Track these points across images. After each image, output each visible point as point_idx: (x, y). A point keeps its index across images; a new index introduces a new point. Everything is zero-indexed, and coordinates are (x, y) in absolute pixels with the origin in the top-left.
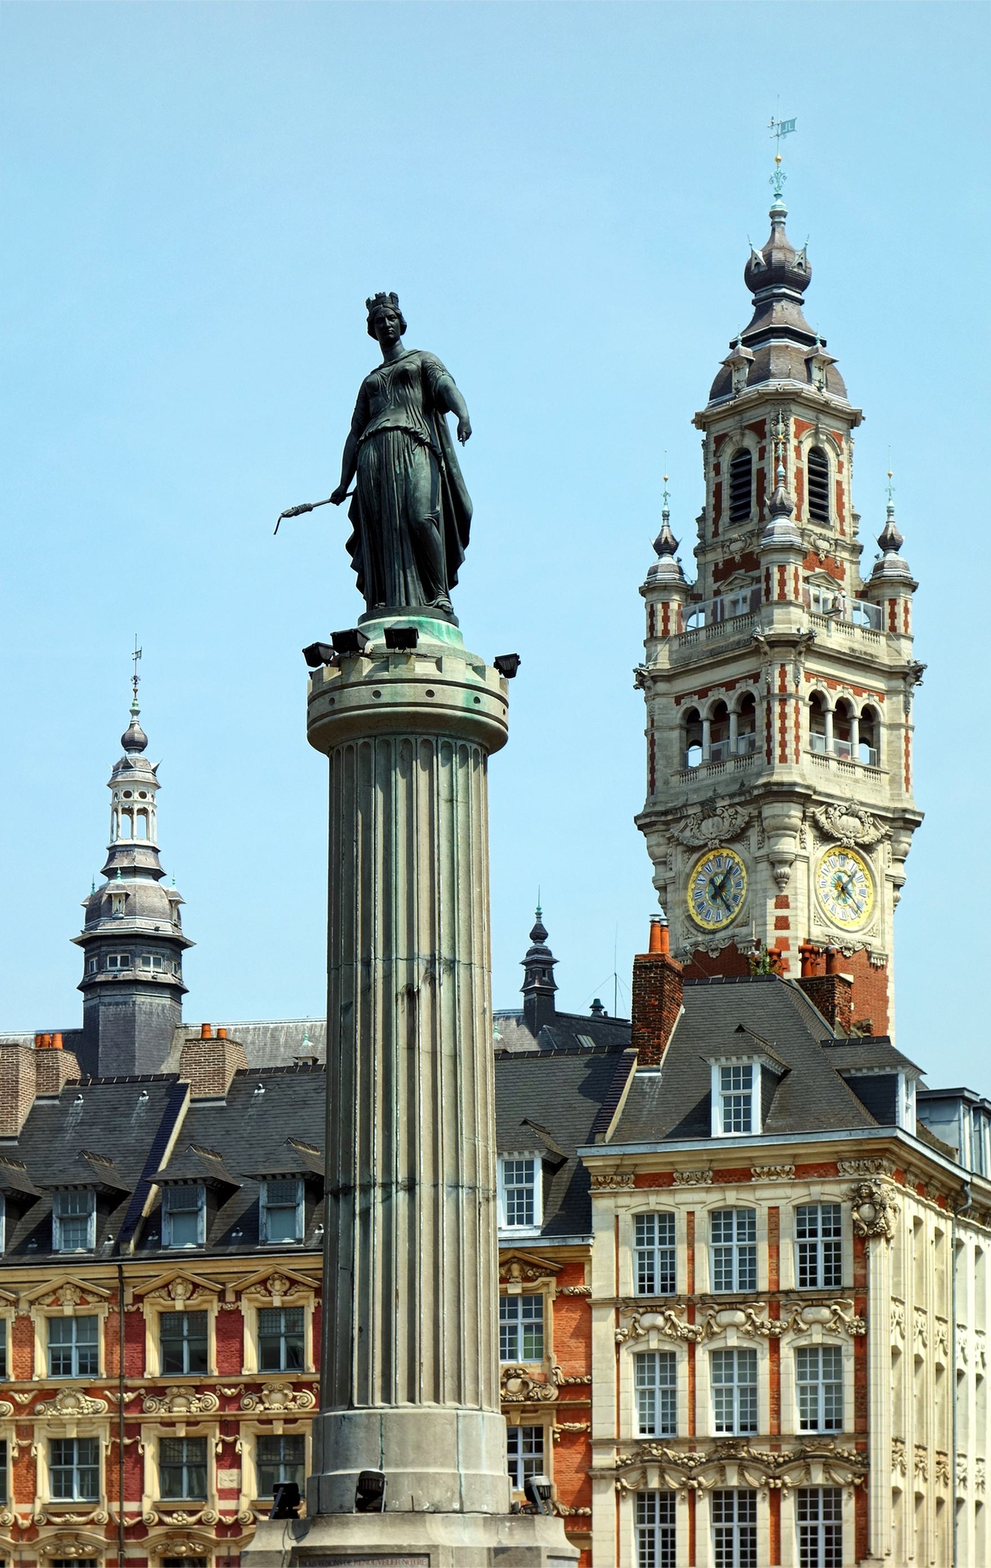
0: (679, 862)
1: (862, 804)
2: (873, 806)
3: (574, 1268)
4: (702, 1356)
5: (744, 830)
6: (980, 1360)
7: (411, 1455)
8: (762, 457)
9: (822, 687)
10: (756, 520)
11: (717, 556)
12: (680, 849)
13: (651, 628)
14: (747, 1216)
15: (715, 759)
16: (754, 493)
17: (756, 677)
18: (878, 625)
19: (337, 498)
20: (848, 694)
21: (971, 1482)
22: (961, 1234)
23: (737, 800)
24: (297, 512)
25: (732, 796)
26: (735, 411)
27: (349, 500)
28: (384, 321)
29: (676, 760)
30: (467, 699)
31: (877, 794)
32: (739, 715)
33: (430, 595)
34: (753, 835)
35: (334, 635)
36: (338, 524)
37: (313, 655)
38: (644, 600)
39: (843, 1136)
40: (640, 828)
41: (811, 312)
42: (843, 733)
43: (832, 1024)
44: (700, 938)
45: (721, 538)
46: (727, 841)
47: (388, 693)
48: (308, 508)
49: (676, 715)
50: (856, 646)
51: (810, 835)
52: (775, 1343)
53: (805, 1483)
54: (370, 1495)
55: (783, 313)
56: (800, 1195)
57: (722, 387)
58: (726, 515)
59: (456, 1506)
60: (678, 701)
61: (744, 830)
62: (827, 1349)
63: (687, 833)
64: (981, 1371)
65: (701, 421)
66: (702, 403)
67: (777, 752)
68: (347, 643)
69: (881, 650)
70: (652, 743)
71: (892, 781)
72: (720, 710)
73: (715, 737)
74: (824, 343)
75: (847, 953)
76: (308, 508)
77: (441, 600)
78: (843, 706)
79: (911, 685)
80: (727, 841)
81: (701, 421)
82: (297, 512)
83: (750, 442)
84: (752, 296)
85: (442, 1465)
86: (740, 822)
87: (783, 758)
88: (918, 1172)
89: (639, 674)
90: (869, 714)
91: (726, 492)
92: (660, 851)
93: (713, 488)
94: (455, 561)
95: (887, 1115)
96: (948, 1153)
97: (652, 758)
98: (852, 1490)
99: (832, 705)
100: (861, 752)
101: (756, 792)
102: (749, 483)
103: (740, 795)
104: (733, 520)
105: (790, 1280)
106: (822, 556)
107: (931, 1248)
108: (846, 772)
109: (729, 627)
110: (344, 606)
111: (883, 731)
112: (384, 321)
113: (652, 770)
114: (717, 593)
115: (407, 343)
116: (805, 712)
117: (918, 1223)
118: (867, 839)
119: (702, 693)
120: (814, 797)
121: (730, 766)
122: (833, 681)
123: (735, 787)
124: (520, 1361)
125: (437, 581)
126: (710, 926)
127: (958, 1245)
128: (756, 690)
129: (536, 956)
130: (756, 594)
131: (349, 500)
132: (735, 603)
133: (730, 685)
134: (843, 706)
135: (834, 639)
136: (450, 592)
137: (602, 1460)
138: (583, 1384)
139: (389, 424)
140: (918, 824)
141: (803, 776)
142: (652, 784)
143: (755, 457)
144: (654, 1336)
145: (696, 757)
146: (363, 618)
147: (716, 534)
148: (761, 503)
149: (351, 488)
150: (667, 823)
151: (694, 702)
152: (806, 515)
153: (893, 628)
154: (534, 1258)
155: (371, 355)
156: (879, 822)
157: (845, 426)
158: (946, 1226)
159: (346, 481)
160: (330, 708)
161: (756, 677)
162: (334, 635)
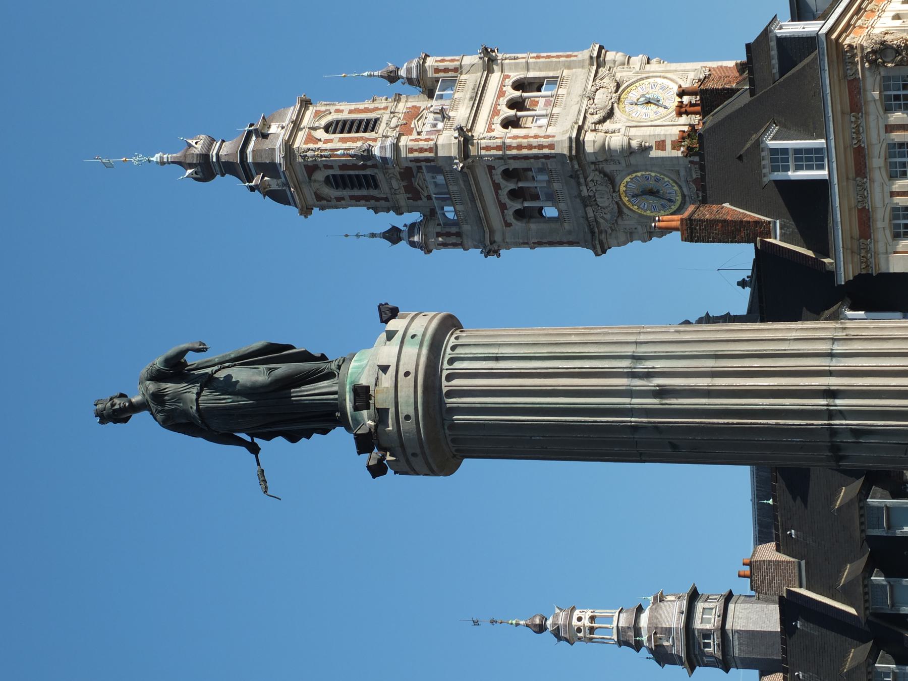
11: (402, 198)
20: (503, 101)
51: (608, 125)
72: (515, 194)
73: (536, 197)
91: (357, 192)
101: (576, 166)
104: (376, 186)
118: (612, 87)
119: (503, 207)
122: (495, 112)
133: (497, 187)
143: (331, 172)
147: (386, 199)
148: (364, 167)
152: (373, 135)
153: (456, 70)
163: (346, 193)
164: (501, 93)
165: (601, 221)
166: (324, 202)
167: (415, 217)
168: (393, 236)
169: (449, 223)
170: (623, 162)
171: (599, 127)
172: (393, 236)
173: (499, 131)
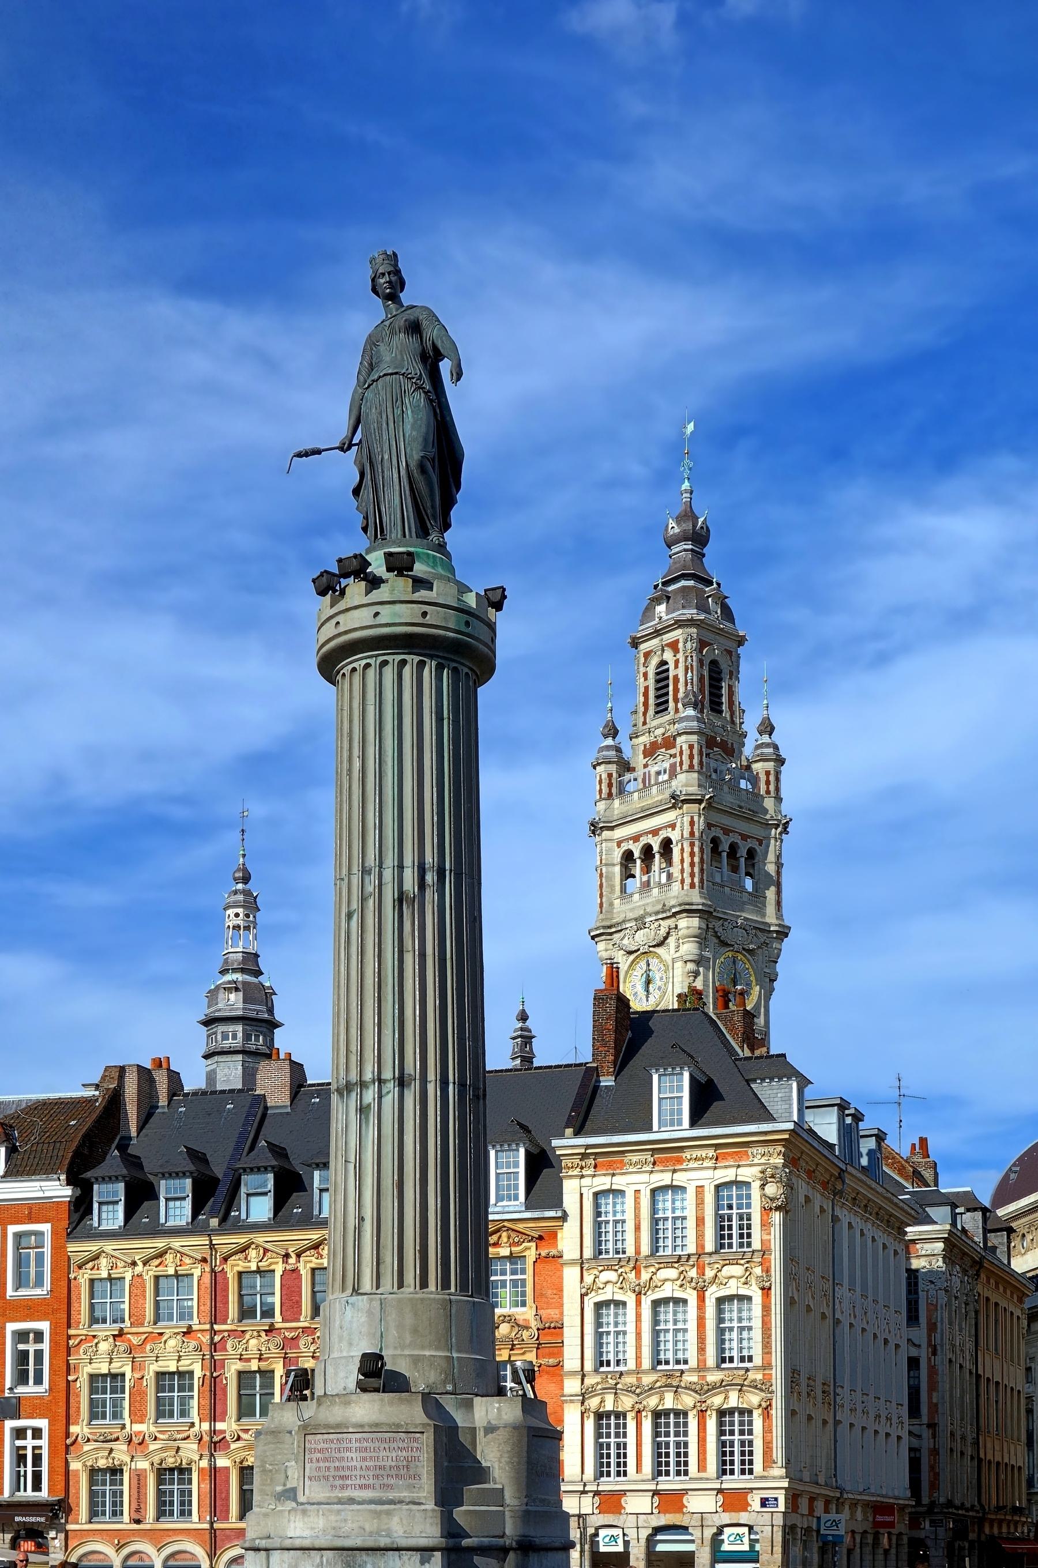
5: (666, 938)
8: (676, 667)
9: (719, 833)
10: (672, 713)
16: (671, 693)
17: (673, 826)
20: (737, 839)
23: (660, 916)
25: (657, 913)
34: (671, 940)
42: (735, 869)
72: (647, 850)
78: (733, 848)
83: (668, 656)
86: (663, 932)
91: (652, 694)
101: (674, 910)
102: (667, 686)
104: (657, 713)
109: (654, 789)
114: (646, 766)
118: (751, 947)
119: (636, 839)
122: (727, 832)
123: (659, 907)
128: (674, 836)
130: (673, 766)
132: (658, 773)
133: (655, 832)
134: (733, 848)
143: (671, 666)
147: (645, 723)
148: (676, 700)
164: (745, 837)
165: (622, 934)
170: (678, 955)
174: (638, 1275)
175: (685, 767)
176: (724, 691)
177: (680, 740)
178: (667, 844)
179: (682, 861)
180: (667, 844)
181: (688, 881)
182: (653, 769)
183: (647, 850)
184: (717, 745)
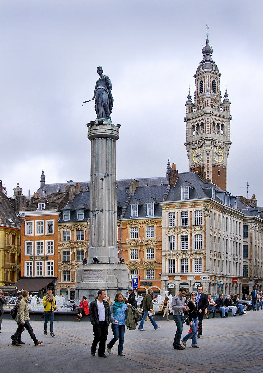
0: (191, 151)
1: (221, 141)
2: (223, 141)
3: (158, 222)
4: (179, 236)
5: (202, 146)
6: (227, 236)
7: (102, 254)
8: (205, 82)
9: (215, 121)
10: (204, 93)
11: (197, 99)
12: (192, 149)
13: (187, 111)
14: (187, 213)
15: (197, 133)
16: (203, 88)
17: (204, 119)
18: (224, 110)
19: (93, 99)
20: (219, 122)
21: (225, 257)
22: (224, 215)
23: (201, 140)
24: (86, 102)
25: (200, 140)
26: (200, 74)
27: (95, 100)
28: (100, 71)
29: (191, 134)
30: (111, 132)
31: (224, 139)
32: (201, 126)
33: (107, 114)
34: (203, 146)
35: (91, 122)
36: (93, 104)
37: (88, 125)
38: (186, 107)
39: (202, 199)
40: (185, 145)
41: (214, 57)
42: (219, 129)
43: (203, 180)
44: (195, 164)
45: (198, 96)
46: (199, 147)
47: (99, 131)
48: (88, 101)
49: (191, 126)
50: (220, 114)
51: (213, 146)
52: (191, 234)
53: (196, 258)
54: (96, 261)
55: (208, 58)
56: (182, 210)
57: (198, 70)
58: (199, 92)
59: (109, 262)
60: (212, 119)
61: (202, 146)
62: (200, 235)
63: (193, 146)
64: (227, 238)
65: (195, 76)
66: (195, 73)
67: (207, 132)
68: (93, 123)
69: (225, 114)
70: (187, 131)
71: (226, 137)
72: (198, 125)
73: (197, 130)
74: (215, 62)
75: (219, 166)
76: (88, 101)
77: (108, 116)
78: (218, 124)
79: (230, 120)
80: (199, 147)
81: (195, 76)
82: (86, 102)
83: (203, 80)
84: (203, 55)
85: (107, 256)
86: (201, 144)
87: (208, 133)
88: (215, 205)
89: (185, 119)
90: (223, 125)
91: (199, 88)
92: (188, 149)
93: (197, 87)
94: (111, 109)
95: (210, 196)
96: (221, 202)
97: (187, 133)
98: (203, 259)
99: (216, 124)
100: (222, 132)
101: (204, 139)
102: (203, 86)
103: (201, 140)
104: (200, 93)
105: (193, 223)
106: (215, 99)
107: (218, 218)
108: (219, 135)
109: (199, 111)
110: (93, 117)
111: (225, 128)
112: (100, 71)
113: (187, 136)
114: (198, 105)
115: (103, 74)
116: (212, 125)
117: (215, 213)
118: (222, 147)
119: (195, 122)
120: (213, 140)
121: (200, 135)
122: (217, 120)
123: (200, 138)
124: (135, 238)
125: (107, 112)
126: (196, 162)
127: (223, 217)
128: (204, 122)
129: (168, 168)
130: (204, 105)
131: (95, 100)
132: (200, 107)
133: (199, 121)
134: (218, 124)
135: (216, 112)
136: (110, 114)
137: (164, 254)
138: (160, 241)
139: (100, 88)
140: (231, 144)
141: (211, 136)
142: (187, 138)
143: (204, 82)
144: (184, 232)
145: (194, 133)
146: (96, 119)
147: (197, 95)
148: (205, 90)
149: (95, 98)
150: (189, 145)
151: (194, 124)
152: (212, 92)
153: (227, 111)
154: (153, 220)
155: (98, 77)
156: (224, 144)
157: (219, 76)
158: (221, 214)
159: (94, 97)
160: (90, 134)
161: (204, 119)
162: (91, 122)
163: (199, 86)
164: (221, 121)
165: (192, 145)
166: (197, 81)
167: (193, 102)
168: (189, 97)
169: (192, 110)
170: (205, 149)
171: (212, 144)
172: (189, 97)
173: (212, 121)
174: (178, 230)
175: (206, 106)
176: (216, 87)
177: (205, 100)
178: (202, 123)
179: (206, 128)
180: (202, 123)
181: (207, 132)
182: (199, 106)
183: (198, 125)
184: (215, 100)
